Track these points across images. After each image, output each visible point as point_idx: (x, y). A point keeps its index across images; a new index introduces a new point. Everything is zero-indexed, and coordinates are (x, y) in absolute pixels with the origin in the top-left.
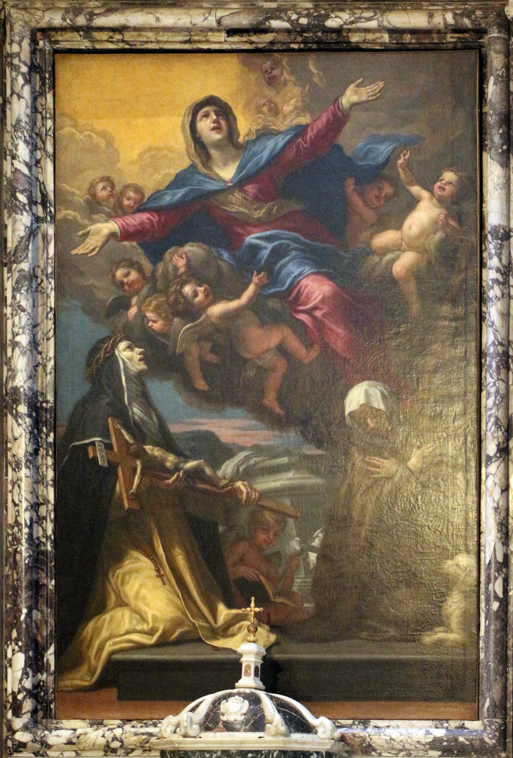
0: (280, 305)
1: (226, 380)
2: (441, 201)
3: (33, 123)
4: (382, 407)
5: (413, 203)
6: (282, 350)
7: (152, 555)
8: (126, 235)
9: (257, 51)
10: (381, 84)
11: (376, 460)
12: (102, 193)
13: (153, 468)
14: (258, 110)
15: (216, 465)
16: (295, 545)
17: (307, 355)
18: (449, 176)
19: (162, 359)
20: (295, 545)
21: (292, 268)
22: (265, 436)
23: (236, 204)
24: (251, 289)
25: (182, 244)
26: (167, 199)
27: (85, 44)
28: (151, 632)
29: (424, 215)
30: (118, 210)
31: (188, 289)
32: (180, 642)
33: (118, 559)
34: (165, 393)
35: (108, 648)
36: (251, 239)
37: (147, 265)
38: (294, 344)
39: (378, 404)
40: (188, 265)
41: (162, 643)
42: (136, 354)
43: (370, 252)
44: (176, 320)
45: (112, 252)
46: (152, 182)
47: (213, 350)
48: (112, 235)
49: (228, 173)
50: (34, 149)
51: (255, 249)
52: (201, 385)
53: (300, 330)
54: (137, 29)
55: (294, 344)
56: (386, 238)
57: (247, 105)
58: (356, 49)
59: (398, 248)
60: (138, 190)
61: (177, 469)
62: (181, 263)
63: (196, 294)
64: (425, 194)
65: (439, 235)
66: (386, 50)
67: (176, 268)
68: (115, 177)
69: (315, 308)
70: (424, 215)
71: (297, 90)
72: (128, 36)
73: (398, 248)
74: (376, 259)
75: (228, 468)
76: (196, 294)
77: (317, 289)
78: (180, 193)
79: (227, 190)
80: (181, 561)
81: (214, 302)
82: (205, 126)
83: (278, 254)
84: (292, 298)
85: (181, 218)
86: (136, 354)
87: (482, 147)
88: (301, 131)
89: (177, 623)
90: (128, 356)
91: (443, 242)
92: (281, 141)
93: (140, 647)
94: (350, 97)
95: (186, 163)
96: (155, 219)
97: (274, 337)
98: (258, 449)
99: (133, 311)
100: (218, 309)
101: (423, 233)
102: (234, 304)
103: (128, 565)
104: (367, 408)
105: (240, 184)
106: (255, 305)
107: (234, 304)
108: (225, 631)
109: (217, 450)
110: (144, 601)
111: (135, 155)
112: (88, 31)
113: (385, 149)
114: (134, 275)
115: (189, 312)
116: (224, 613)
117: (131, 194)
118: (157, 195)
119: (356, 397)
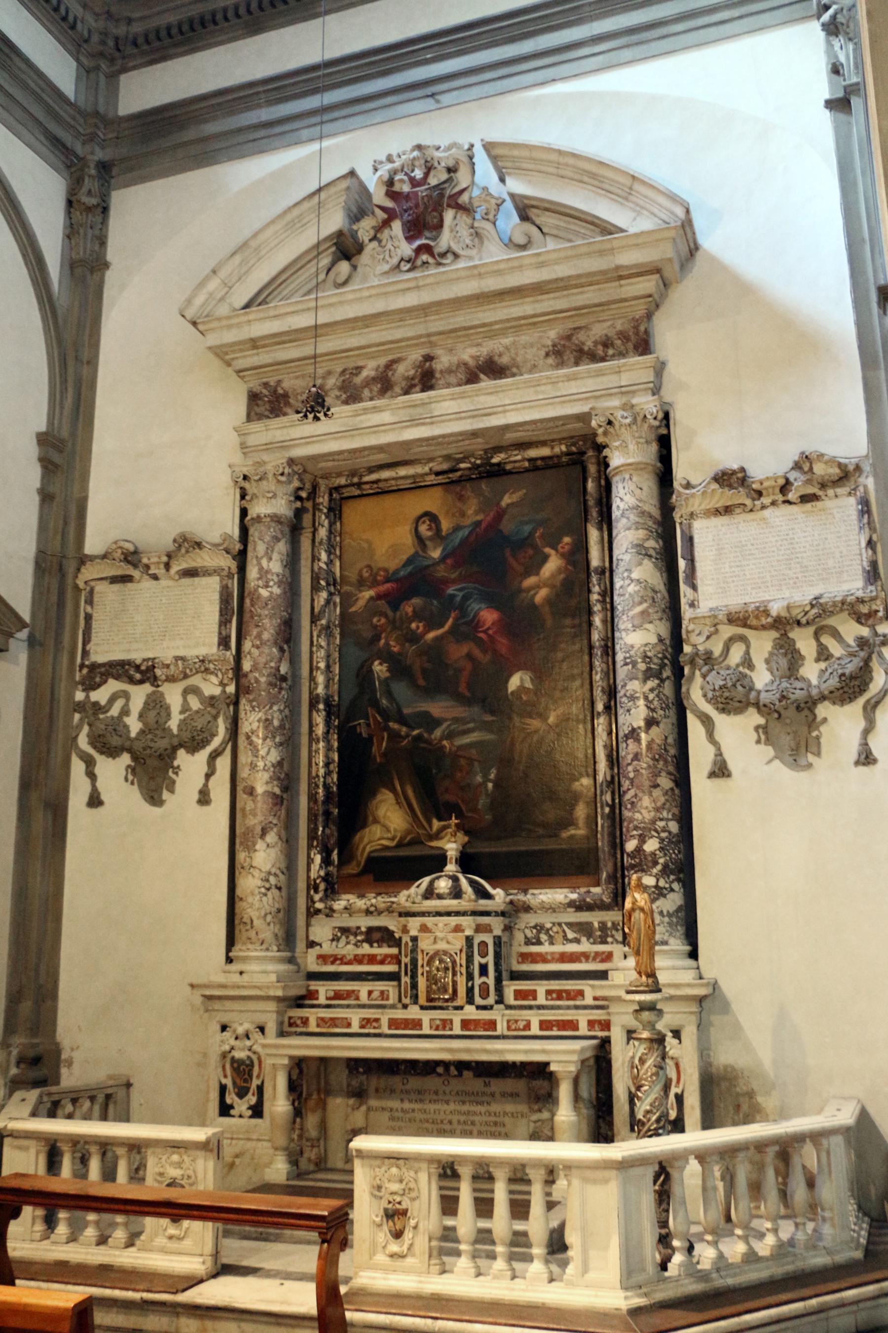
0: (467, 629)
1: (436, 678)
2: (563, 556)
3: (329, 539)
4: (531, 687)
5: (545, 558)
6: (469, 656)
7: (393, 790)
8: (379, 597)
9: (452, 482)
10: (524, 491)
11: (528, 721)
12: (366, 574)
13: (394, 736)
14: (453, 515)
15: (431, 731)
16: (479, 779)
17: (484, 658)
18: (567, 540)
19: (400, 669)
20: (479, 779)
21: (474, 606)
22: (460, 711)
23: (441, 572)
24: (451, 621)
25: (410, 599)
26: (402, 573)
27: (357, 492)
28: (393, 839)
29: (553, 565)
30: (375, 583)
31: (414, 625)
32: (411, 843)
33: (374, 793)
34: (401, 690)
35: (368, 849)
36: (450, 591)
37: (390, 613)
38: (477, 653)
39: (528, 685)
40: (414, 611)
41: (400, 845)
42: (384, 667)
43: (520, 591)
44: (407, 644)
45: (371, 608)
46: (393, 565)
47: (429, 661)
48: (371, 598)
49: (436, 554)
50: (329, 553)
51: (452, 597)
52: (421, 682)
53: (479, 642)
54: (386, 480)
55: (477, 653)
56: (531, 581)
57: (447, 512)
58: (510, 473)
59: (538, 587)
60: (386, 570)
61: (407, 736)
62: (409, 610)
63: (418, 627)
64: (553, 552)
65: (562, 576)
66: (527, 470)
67: (407, 614)
68: (373, 565)
69: (489, 629)
70: (553, 565)
71: (475, 501)
72: (381, 485)
73: (538, 587)
74: (524, 595)
75: (438, 733)
76: (418, 627)
77: (489, 616)
78: (409, 569)
79: (436, 563)
80: (410, 793)
81: (428, 631)
82: (423, 529)
83: (465, 598)
84: (475, 624)
85: (411, 583)
86: (384, 667)
87: (586, 520)
88: (478, 524)
89: (408, 832)
90: (379, 669)
91: (565, 579)
92: (466, 532)
93: (386, 848)
94: (506, 500)
95: (412, 551)
96: (394, 585)
97: (464, 649)
98: (456, 720)
99: (383, 641)
100: (431, 635)
101: (553, 576)
102: (441, 631)
103: (379, 797)
104: (522, 688)
105: (443, 559)
106: (453, 631)
107: (441, 631)
108: (437, 836)
109: (431, 722)
110: (390, 819)
111: (384, 551)
112: (359, 485)
113: (527, 528)
114: (383, 620)
115: (413, 638)
116: (436, 824)
117: (382, 573)
118: (397, 571)
119: (514, 682)
